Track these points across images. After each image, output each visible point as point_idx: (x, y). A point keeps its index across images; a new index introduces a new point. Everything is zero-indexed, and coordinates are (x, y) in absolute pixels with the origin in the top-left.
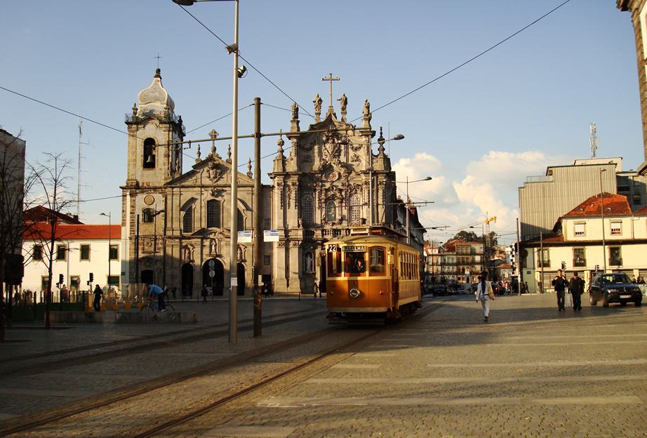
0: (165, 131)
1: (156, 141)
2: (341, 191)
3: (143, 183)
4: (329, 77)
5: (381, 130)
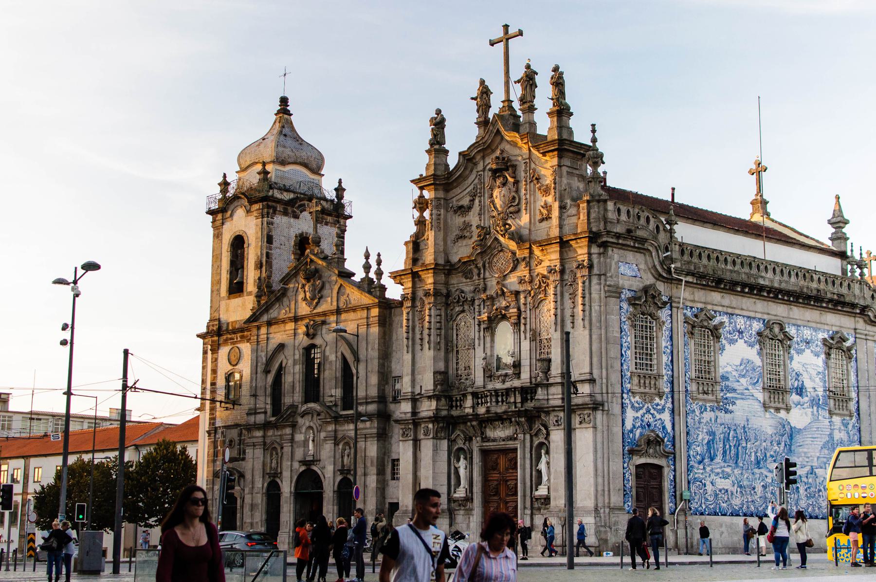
0: (257, 218)
1: (246, 239)
3: (228, 324)
4: (500, 34)
5: (594, 131)
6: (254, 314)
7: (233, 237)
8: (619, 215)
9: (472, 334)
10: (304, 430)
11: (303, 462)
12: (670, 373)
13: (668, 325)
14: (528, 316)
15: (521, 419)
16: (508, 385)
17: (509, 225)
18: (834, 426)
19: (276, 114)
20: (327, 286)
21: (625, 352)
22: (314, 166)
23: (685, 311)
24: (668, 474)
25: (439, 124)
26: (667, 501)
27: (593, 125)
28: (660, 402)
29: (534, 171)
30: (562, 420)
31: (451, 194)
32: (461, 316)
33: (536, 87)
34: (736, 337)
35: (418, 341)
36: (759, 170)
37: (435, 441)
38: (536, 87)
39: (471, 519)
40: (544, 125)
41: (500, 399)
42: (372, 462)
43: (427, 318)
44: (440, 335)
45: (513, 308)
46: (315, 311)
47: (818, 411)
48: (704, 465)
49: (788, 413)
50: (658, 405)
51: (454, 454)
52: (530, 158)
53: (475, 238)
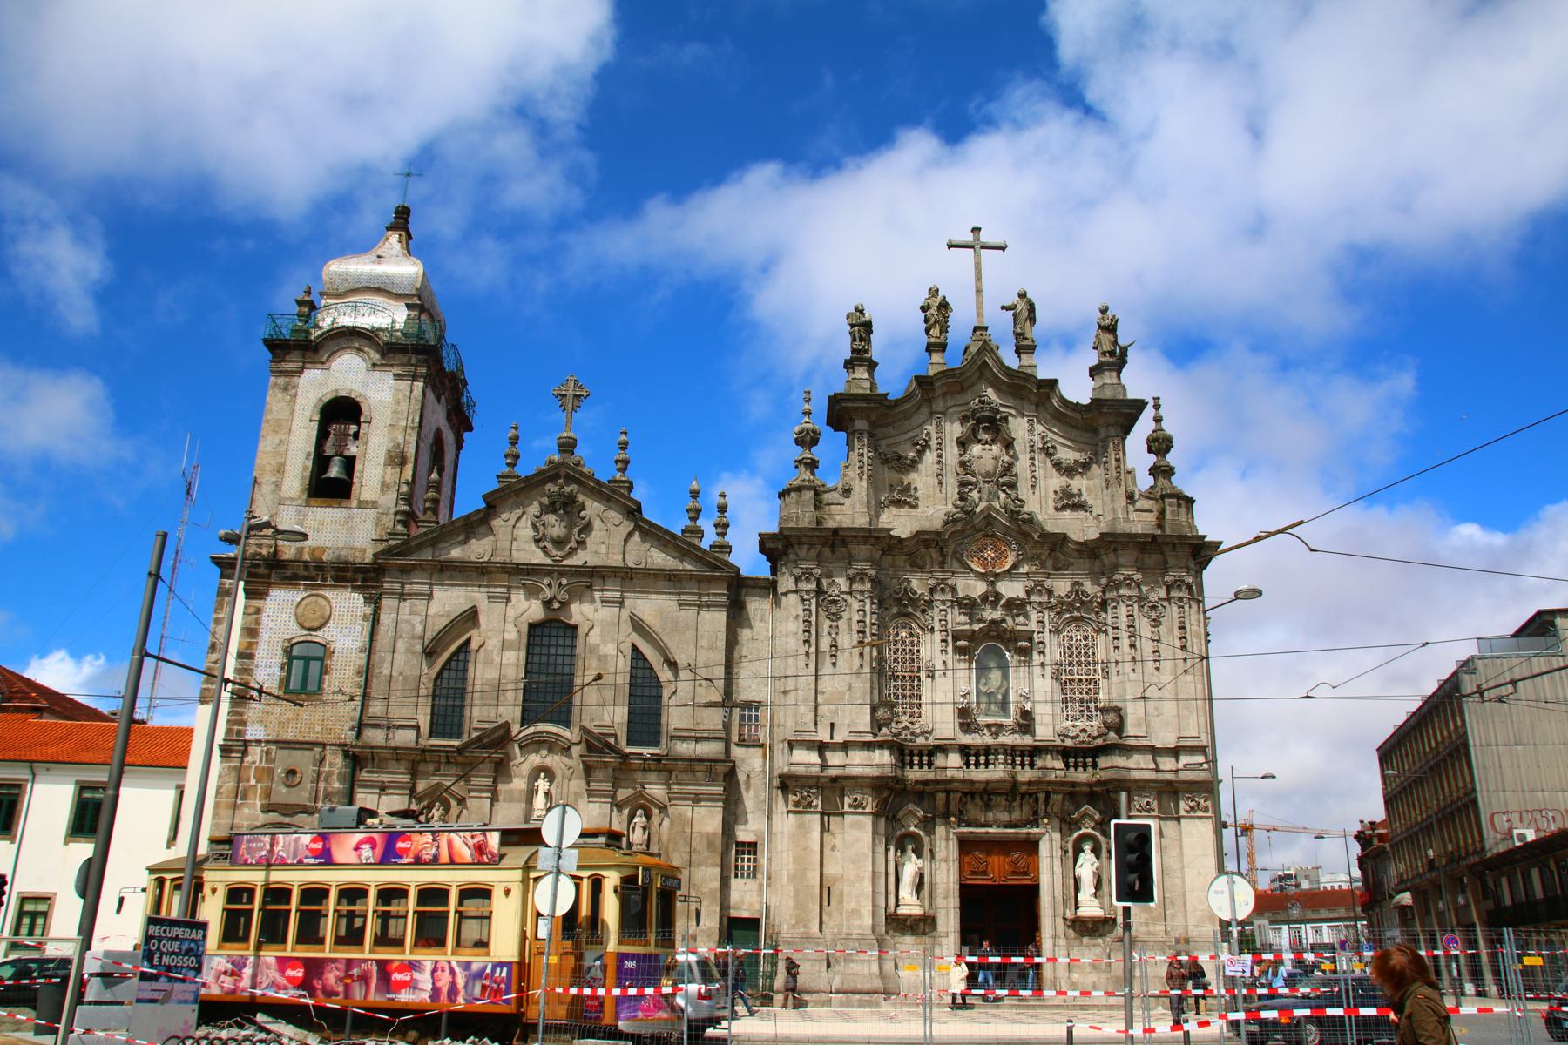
0: (398, 377)
4: (969, 238)
10: (526, 769)
14: (1047, 641)
20: (597, 523)
27: (1159, 399)
41: (1018, 759)
42: (710, 845)
46: (564, 563)
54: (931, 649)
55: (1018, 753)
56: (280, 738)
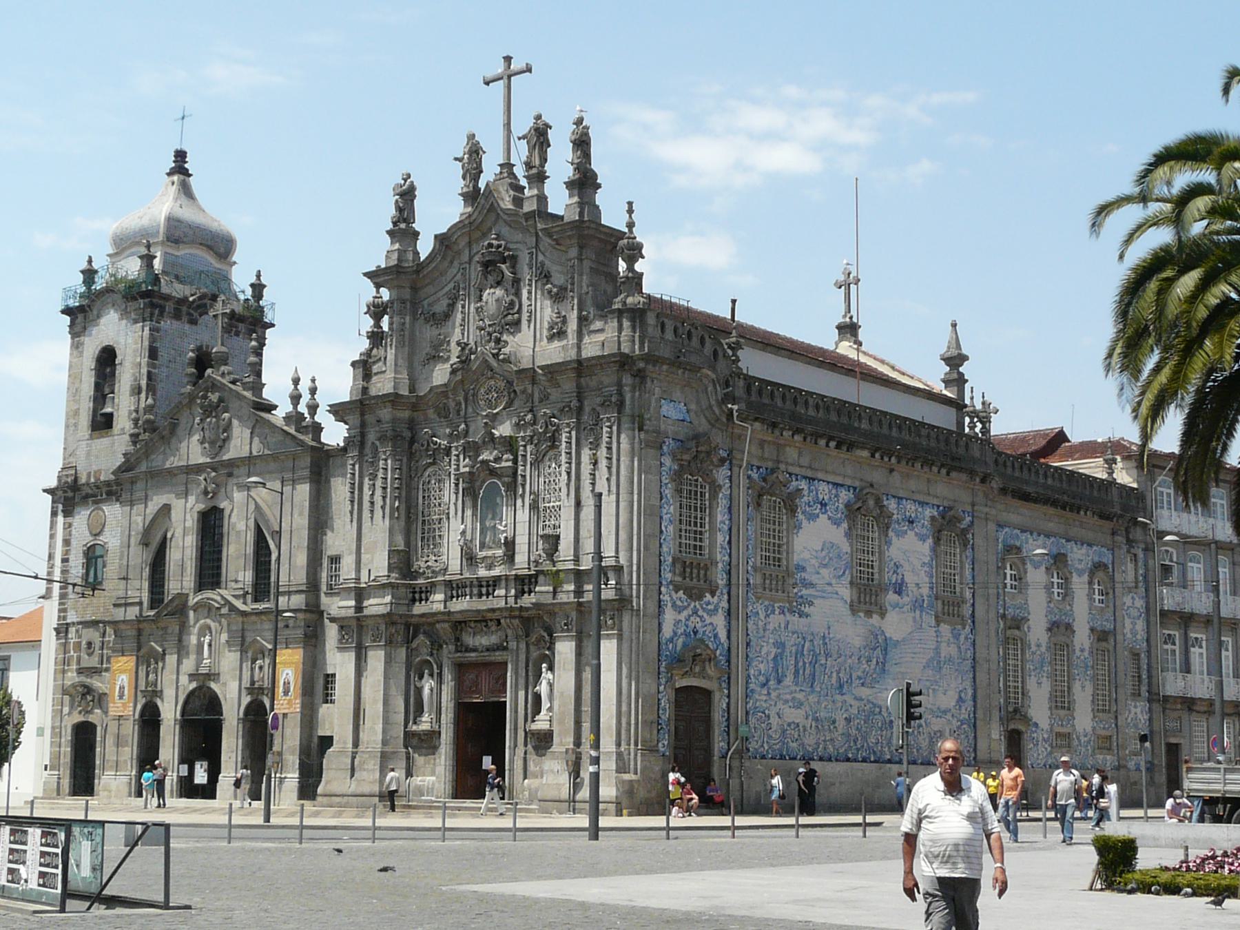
2: (510, 444)
4: (500, 69)
5: (630, 211)
6: (127, 461)
7: (99, 348)
8: (663, 330)
9: (446, 499)
11: (192, 677)
12: (727, 558)
13: (725, 491)
15: (513, 621)
16: (496, 572)
17: (506, 342)
18: (942, 637)
19: (169, 174)
21: (666, 527)
22: (222, 250)
23: (750, 472)
24: (720, 703)
25: (407, 196)
26: (716, 741)
28: (711, 600)
29: (543, 264)
30: (574, 623)
31: (422, 294)
32: (430, 470)
33: (549, 146)
34: (818, 511)
35: (366, 505)
36: (847, 284)
37: (388, 648)
38: (549, 146)
39: (438, 761)
40: (559, 201)
41: (484, 590)
43: (380, 475)
44: (399, 498)
45: (506, 461)
47: (921, 617)
48: (769, 689)
49: (882, 618)
50: (708, 603)
51: (416, 670)
52: (537, 245)
53: (454, 360)
54: (449, 495)
55: (484, 583)
56: (83, 620)
